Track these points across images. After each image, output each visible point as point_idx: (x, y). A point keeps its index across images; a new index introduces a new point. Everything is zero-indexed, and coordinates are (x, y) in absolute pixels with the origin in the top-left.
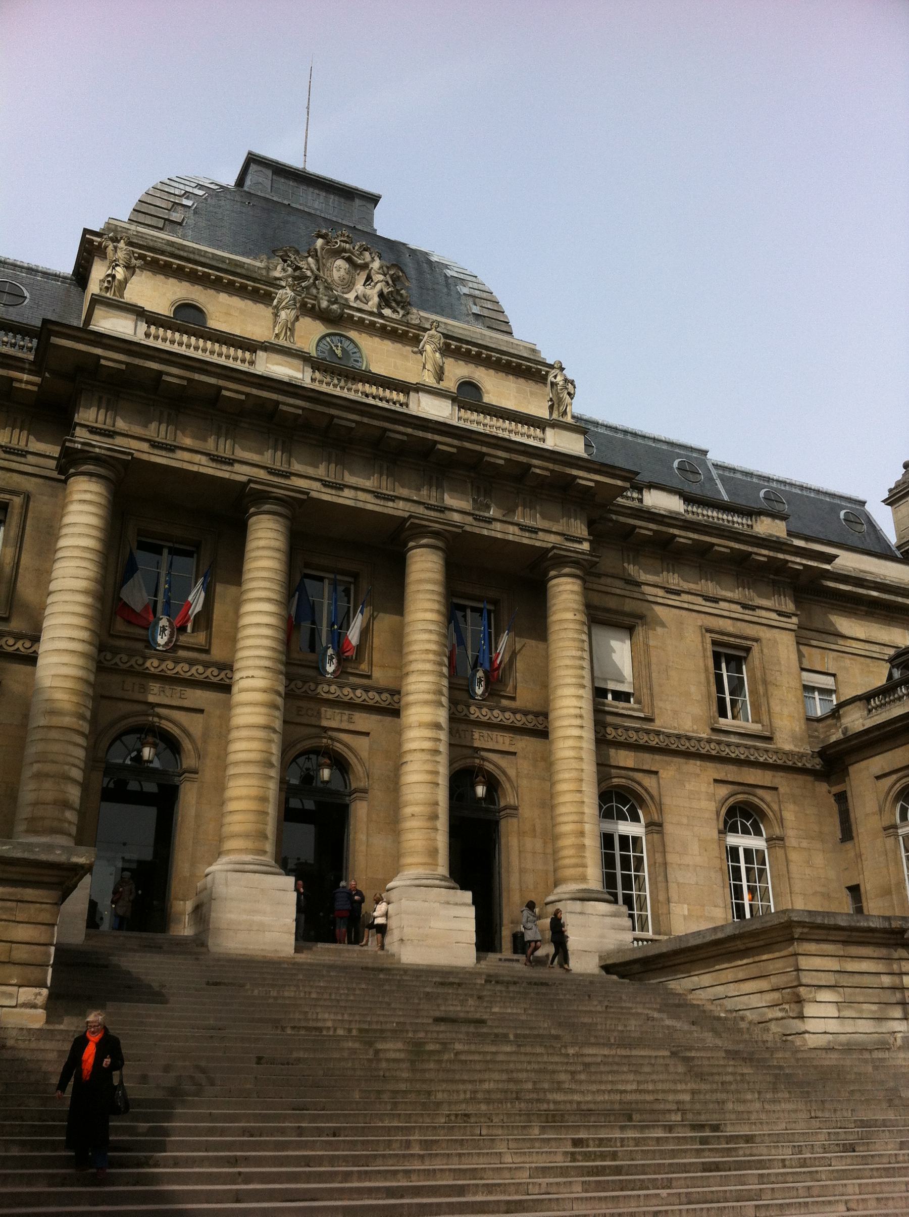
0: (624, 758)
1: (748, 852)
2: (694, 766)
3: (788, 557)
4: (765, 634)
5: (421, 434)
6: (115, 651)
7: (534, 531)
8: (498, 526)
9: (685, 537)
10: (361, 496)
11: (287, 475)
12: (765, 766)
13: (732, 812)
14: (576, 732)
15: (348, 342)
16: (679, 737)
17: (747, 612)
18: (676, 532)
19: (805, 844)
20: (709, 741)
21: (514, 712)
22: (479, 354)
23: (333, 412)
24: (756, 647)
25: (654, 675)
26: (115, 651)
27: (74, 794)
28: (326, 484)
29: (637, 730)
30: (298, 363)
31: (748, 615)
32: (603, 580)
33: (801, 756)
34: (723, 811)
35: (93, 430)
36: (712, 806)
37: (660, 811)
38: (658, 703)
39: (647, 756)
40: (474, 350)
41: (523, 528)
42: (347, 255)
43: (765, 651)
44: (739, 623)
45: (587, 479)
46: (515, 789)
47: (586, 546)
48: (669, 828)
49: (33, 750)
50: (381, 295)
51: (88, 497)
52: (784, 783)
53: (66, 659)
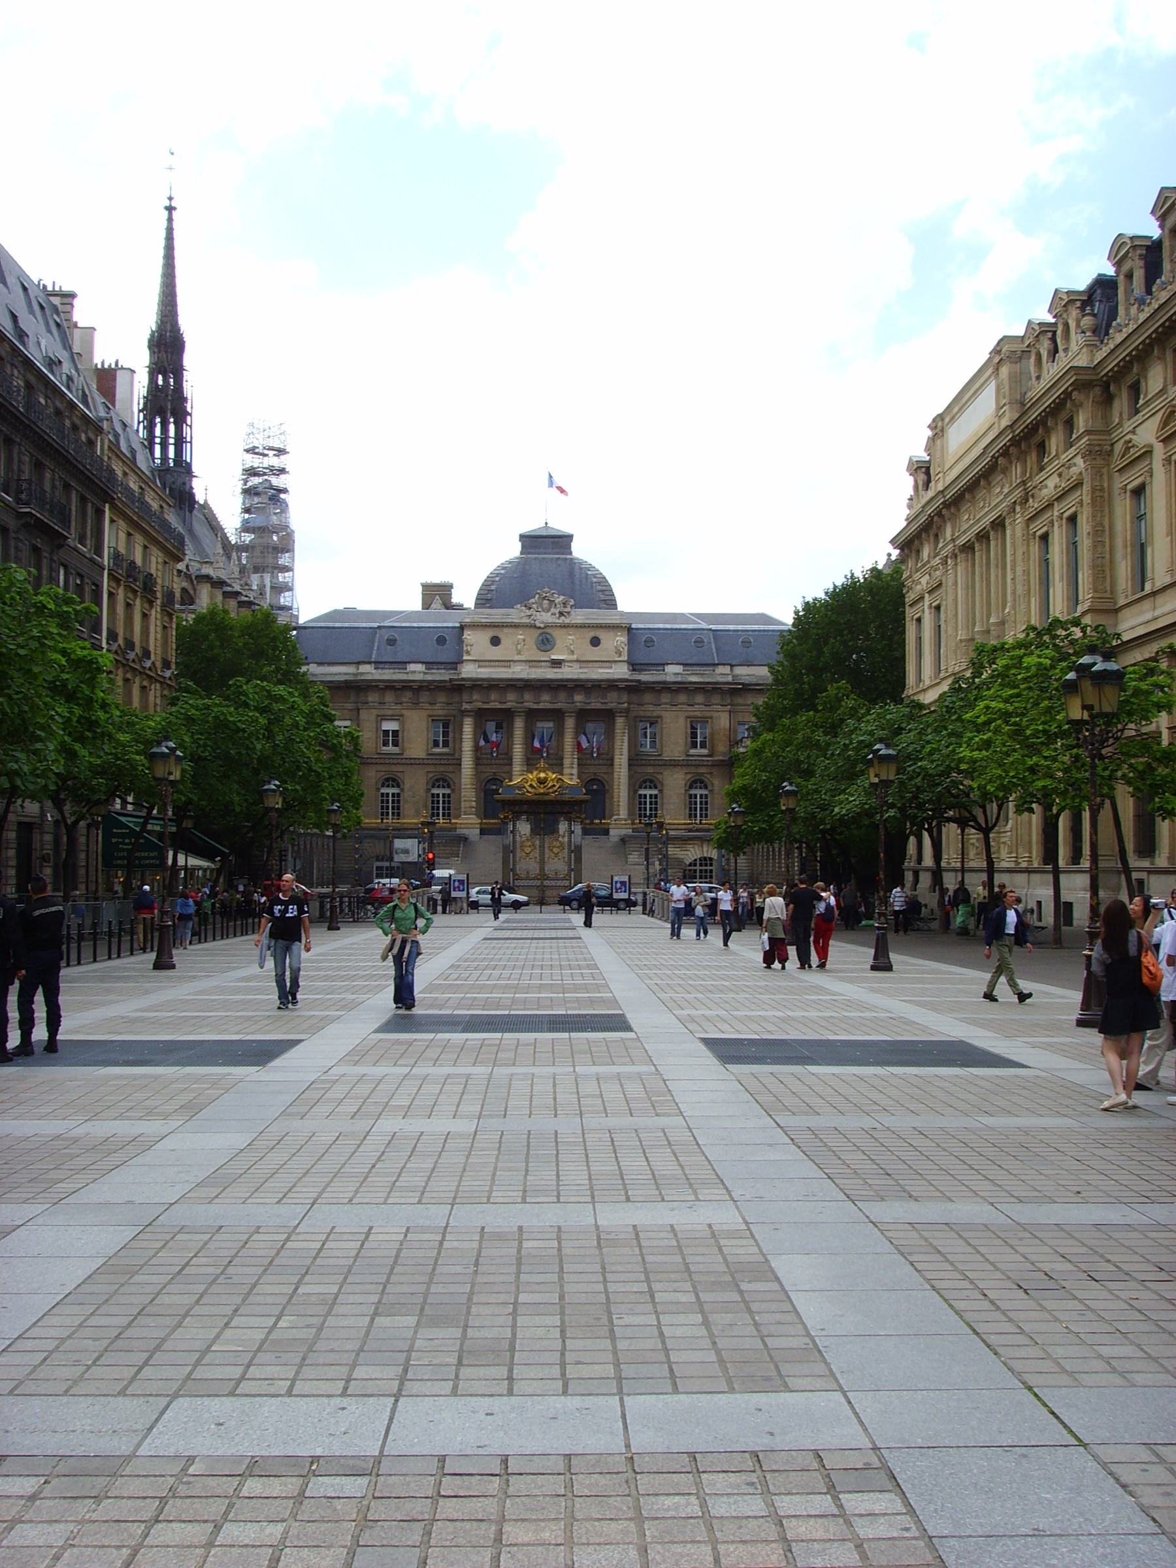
0: (650, 770)
1: (701, 796)
2: (676, 769)
4: (715, 715)
9: (674, 687)
13: (695, 782)
27: (474, 804)
31: (707, 708)
45: (622, 685)
52: (714, 770)
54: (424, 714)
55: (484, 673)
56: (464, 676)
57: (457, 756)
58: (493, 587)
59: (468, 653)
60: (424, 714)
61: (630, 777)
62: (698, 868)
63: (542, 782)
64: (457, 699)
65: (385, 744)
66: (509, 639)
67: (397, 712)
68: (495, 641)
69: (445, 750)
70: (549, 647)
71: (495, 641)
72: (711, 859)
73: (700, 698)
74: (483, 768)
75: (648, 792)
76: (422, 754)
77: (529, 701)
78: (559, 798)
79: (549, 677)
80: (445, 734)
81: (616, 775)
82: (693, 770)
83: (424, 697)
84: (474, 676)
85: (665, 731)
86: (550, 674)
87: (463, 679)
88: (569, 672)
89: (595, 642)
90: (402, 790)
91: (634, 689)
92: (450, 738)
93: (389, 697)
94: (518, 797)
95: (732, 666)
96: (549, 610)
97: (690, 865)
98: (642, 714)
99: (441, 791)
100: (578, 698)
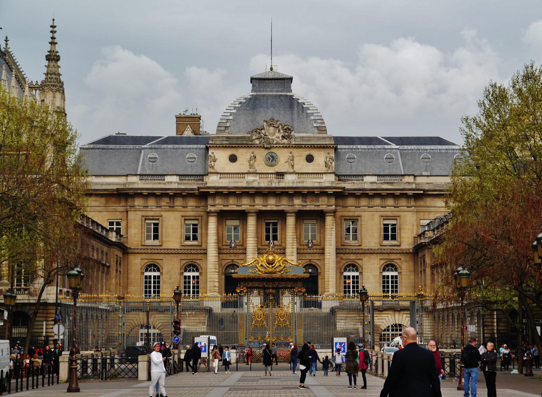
0: (353, 257)
1: (392, 277)
2: (374, 256)
3: (407, 192)
4: (402, 214)
5: (284, 190)
6: (224, 249)
7: (319, 206)
8: (309, 206)
9: (371, 193)
10: (272, 206)
11: (254, 206)
12: (396, 253)
13: (387, 266)
14: (328, 257)
16: (368, 249)
18: (368, 192)
19: (408, 273)
20: (378, 249)
21: (320, 249)
22: (311, 147)
23: (262, 190)
24: (398, 218)
25: (363, 232)
26: (224, 249)
28: (263, 206)
29: (355, 249)
30: (254, 175)
31: (396, 209)
32: (348, 208)
33: (409, 250)
34: (382, 267)
35: (211, 206)
36: (379, 266)
37: (362, 269)
38: (363, 240)
39: (359, 255)
40: (310, 146)
41: (315, 206)
43: (402, 219)
45: (330, 191)
46: (320, 268)
47: (334, 207)
48: (364, 273)
49: (208, 276)
51: (212, 221)
52: (403, 258)
53: (212, 258)
54: (178, 215)
55: (224, 182)
56: (208, 185)
57: (204, 247)
58: (231, 118)
59: (212, 167)
60: (178, 215)
61: (338, 263)
62: (390, 333)
63: (270, 263)
64: (203, 204)
65: (148, 238)
66: (243, 155)
67: (157, 214)
68: (233, 159)
69: (195, 243)
70: (274, 162)
71: (233, 159)
72: (400, 325)
73: (390, 202)
74: (224, 256)
75: (351, 274)
76: (176, 246)
77: (259, 204)
78: (284, 276)
79: (274, 185)
80: (195, 230)
81: (326, 261)
82: (386, 256)
83: (179, 202)
84: (217, 185)
85: (364, 227)
86: (275, 183)
87: (209, 188)
88: (290, 181)
89: (310, 159)
90: (162, 273)
91: (340, 195)
92: (198, 235)
93: (151, 202)
94: (252, 275)
95: (415, 176)
96: (274, 134)
97: (384, 331)
98: (346, 214)
99: (192, 274)
100: (298, 202)
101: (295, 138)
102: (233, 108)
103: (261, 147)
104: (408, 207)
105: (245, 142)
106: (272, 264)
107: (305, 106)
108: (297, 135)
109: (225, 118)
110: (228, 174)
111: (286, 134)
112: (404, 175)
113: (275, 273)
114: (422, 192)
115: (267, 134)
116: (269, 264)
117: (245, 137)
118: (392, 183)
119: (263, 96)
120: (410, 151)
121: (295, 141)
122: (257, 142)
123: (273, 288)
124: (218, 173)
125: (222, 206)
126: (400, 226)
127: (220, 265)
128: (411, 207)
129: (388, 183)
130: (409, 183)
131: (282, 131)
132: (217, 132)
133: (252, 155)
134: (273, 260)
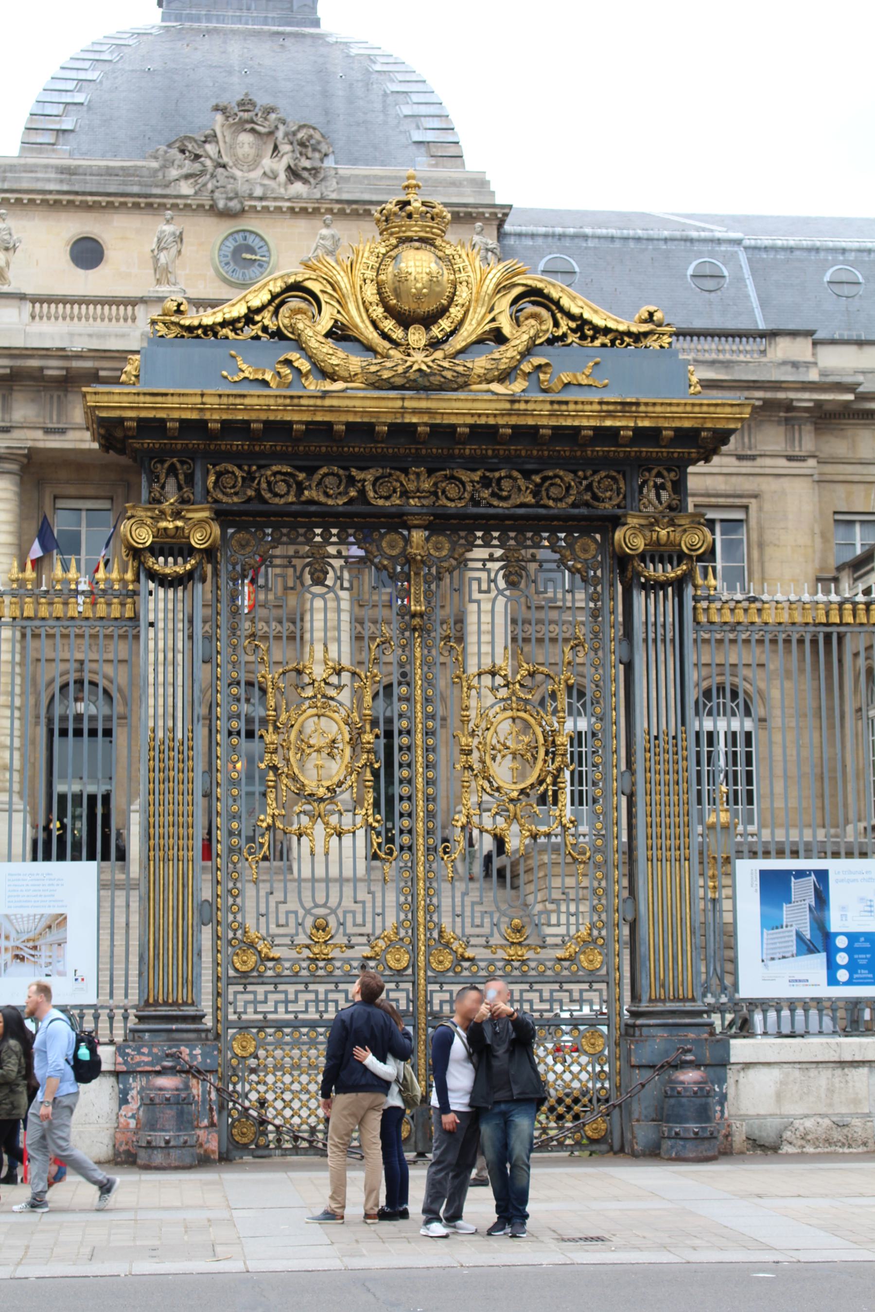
3: (792, 395)
4: (767, 486)
15: (253, 237)
17: (745, 463)
24: (753, 504)
31: (746, 467)
42: (248, 126)
43: (767, 506)
44: (734, 479)
50: (289, 167)
58: (79, 98)
71: (88, 253)
74: (46, 649)
78: (540, 413)
84: (18, 342)
94: (258, 405)
95: (815, 344)
96: (255, 163)
101: (341, 180)
102: (86, 65)
103: (201, 206)
104: (790, 458)
105: (136, 189)
106: (428, 320)
107: (378, 67)
108: (345, 170)
109: (55, 97)
110: (64, 300)
111: (307, 164)
112: (772, 335)
113: (461, 383)
114: (850, 397)
115: (225, 159)
116: (405, 321)
117: (136, 168)
118: (727, 365)
119: (209, 31)
120: (781, 256)
121: (339, 190)
122: (186, 188)
123: (440, 523)
124: (22, 297)
125: (39, 434)
126: (761, 535)
127: (31, 683)
128: (803, 459)
129: (713, 363)
130: (795, 365)
131: (285, 148)
132: (22, 149)
133: (168, 229)
134: (433, 281)
